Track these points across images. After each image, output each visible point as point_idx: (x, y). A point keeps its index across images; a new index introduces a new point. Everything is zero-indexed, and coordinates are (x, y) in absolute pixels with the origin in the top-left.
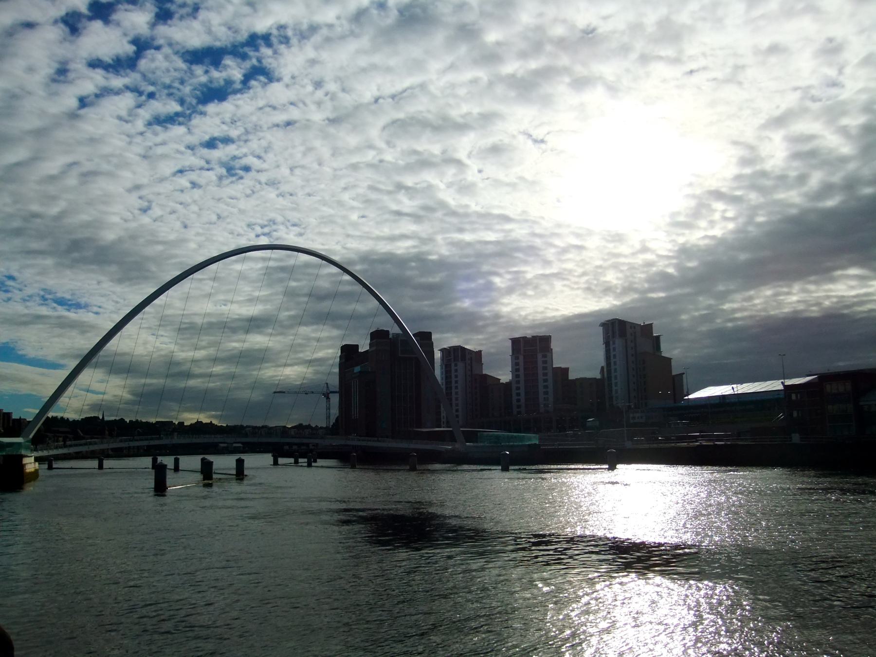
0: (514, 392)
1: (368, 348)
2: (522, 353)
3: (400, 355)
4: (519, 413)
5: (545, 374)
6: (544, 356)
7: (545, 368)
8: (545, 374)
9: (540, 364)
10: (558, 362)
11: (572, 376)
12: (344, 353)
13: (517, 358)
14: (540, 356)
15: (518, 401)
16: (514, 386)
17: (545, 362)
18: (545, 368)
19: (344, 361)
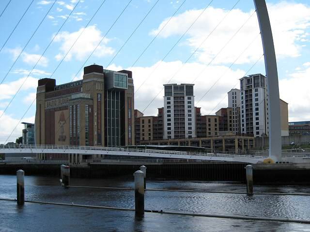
0: (166, 122)
1: (81, 78)
2: (173, 95)
3: (114, 87)
4: (170, 137)
5: (190, 111)
6: (189, 98)
7: (189, 107)
8: (190, 111)
9: (186, 105)
10: (197, 104)
11: (204, 112)
12: (44, 86)
13: (169, 99)
14: (186, 98)
15: (169, 129)
16: (166, 118)
17: (190, 102)
18: (189, 107)
19: (44, 91)
